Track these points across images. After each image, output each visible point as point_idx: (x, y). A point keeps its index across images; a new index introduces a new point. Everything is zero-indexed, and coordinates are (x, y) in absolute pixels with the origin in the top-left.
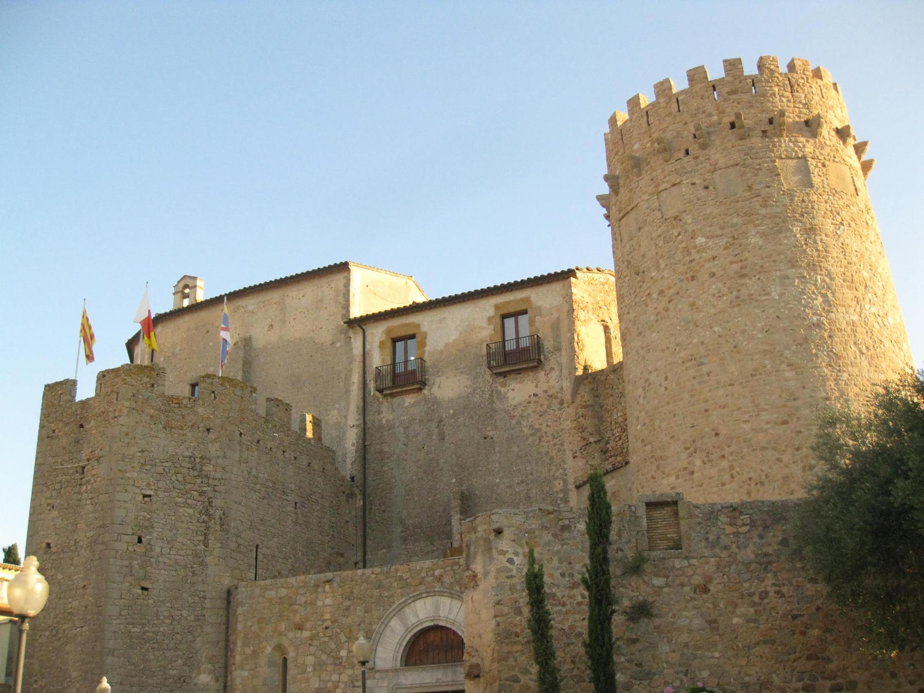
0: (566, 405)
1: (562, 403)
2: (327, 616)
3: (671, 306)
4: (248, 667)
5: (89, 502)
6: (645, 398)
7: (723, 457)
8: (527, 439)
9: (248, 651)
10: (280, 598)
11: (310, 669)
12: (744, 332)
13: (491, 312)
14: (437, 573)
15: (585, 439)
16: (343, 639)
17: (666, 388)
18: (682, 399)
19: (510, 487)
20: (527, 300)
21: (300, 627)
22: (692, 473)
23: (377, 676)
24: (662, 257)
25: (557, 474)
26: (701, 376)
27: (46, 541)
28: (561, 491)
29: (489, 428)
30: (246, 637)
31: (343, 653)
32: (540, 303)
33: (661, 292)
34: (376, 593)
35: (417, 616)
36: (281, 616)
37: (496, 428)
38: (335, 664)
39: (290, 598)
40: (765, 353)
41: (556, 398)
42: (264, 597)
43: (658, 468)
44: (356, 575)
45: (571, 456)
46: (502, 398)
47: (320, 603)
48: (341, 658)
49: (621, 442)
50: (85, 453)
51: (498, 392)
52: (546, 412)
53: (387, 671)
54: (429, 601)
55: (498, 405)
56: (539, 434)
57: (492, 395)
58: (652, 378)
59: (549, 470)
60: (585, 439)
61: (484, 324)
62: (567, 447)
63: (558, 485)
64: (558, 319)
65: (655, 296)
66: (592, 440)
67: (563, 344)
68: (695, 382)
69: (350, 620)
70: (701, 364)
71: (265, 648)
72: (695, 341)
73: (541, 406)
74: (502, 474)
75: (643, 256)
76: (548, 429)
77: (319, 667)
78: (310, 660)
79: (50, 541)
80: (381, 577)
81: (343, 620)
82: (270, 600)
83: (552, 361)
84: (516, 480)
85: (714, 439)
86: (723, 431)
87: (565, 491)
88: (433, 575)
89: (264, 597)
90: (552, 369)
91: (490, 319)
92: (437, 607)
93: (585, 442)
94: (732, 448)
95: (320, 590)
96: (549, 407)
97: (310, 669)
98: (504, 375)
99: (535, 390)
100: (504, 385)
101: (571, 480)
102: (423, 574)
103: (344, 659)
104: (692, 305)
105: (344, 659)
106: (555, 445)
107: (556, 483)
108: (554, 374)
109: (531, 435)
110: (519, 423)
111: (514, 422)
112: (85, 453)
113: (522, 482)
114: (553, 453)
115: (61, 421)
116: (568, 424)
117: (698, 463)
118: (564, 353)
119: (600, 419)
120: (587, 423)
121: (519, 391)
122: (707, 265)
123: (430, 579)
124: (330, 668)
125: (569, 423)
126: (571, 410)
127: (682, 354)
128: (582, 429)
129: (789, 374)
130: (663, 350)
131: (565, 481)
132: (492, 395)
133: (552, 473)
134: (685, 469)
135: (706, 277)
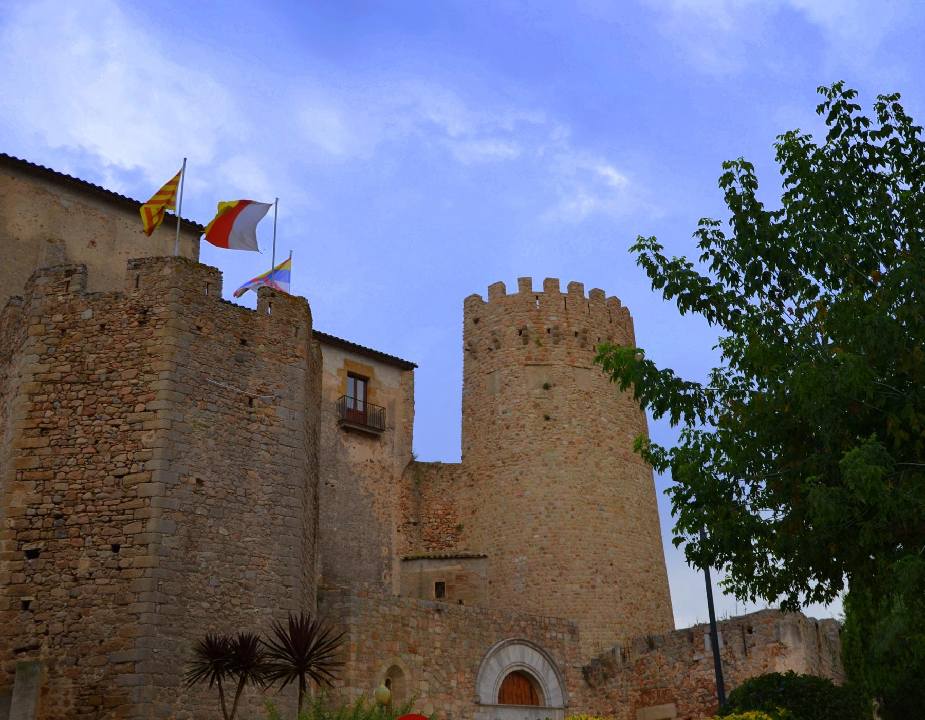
0: (394, 481)
1: (392, 477)
2: (438, 644)
3: (580, 457)
4: (363, 684)
5: (264, 447)
6: (547, 516)
7: (616, 582)
8: (363, 500)
9: (364, 666)
10: (394, 616)
11: (424, 695)
12: (627, 499)
13: (341, 365)
14: (523, 624)
16: (453, 670)
17: (573, 517)
18: (586, 530)
19: (345, 539)
20: (371, 370)
21: (413, 651)
22: (594, 587)
23: (482, 709)
24: (574, 416)
25: (384, 541)
26: (602, 518)
27: (197, 475)
28: (387, 557)
29: (331, 476)
30: (359, 651)
31: (453, 683)
32: (381, 379)
33: (571, 443)
34: (477, 631)
35: (509, 659)
36: (396, 636)
37: (337, 478)
38: (447, 693)
39: (403, 618)
40: (638, 519)
41: (388, 471)
42: (377, 611)
43: (561, 574)
44: (460, 610)
45: (395, 528)
46: (345, 452)
47: (431, 630)
48: (451, 688)
49: (438, 531)
50: (253, 382)
51: (341, 443)
52: (378, 480)
53: (489, 706)
54: (518, 648)
55: (340, 456)
56: (372, 499)
57: (336, 444)
58: (558, 504)
59: (378, 536)
61: (334, 373)
63: (385, 551)
64: (394, 401)
65: (565, 443)
66: (412, 520)
67: (396, 425)
68: (598, 521)
69: (457, 652)
70: (602, 510)
71: (381, 666)
72: (599, 491)
74: (339, 525)
75: (557, 408)
76: (379, 497)
77: (432, 694)
78: (425, 686)
79: (203, 478)
80: (481, 617)
81: (451, 650)
82: (384, 616)
83: (392, 437)
84: (351, 535)
85: (610, 568)
86: (615, 563)
87: (390, 558)
88: (519, 625)
89: (377, 611)
90: (386, 444)
91: (339, 370)
92: (523, 656)
93: (406, 520)
94: (621, 578)
95: (430, 616)
96: (382, 477)
97: (424, 695)
98: (347, 430)
99: (371, 457)
100: (347, 440)
101: (394, 550)
102: (512, 623)
103: (455, 689)
104: (597, 464)
105: (455, 689)
106: (384, 513)
107: (383, 548)
108: (387, 449)
109: (366, 496)
110: (356, 481)
111: (353, 478)
112: (253, 382)
113: (356, 538)
114: (382, 521)
115: (212, 321)
116: (395, 499)
117: (599, 580)
118: (396, 433)
119: (419, 503)
120: (410, 504)
121: (358, 451)
122: (608, 440)
123: (516, 628)
124: (442, 696)
125: (396, 497)
126: (398, 487)
127: (588, 496)
128: (404, 507)
129: (648, 539)
130: (571, 487)
131: (390, 549)
132: (336, 444)
133: (380, 538)
134: (589, 582)
135: (607, 448)
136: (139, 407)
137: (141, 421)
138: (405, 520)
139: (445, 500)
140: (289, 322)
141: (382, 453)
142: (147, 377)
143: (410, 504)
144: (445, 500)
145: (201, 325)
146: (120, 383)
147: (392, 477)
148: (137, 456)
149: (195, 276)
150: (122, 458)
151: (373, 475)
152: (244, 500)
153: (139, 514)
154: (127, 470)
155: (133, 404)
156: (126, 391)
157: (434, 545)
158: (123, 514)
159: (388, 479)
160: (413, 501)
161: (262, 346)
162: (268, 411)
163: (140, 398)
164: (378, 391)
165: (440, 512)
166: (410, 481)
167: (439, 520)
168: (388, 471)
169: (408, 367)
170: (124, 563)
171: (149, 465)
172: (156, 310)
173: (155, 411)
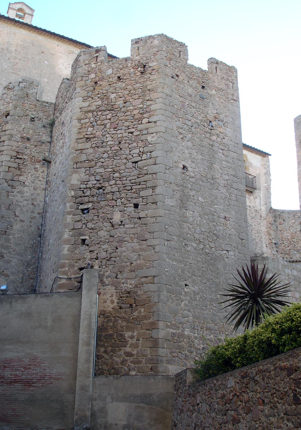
15: (270, 240)
27: (183, 163)
32: (251, 161)
45: (265, 245)
60: (270, 240)
62: (263, 240)
73: (252, 213)
76: (255, 227)
83: (260, 193)
96: (256, 215)
108: (258, 201)
114: (257, 240)
115: (184, 72)
116: (263, 229)
118: (262, 192)
120: (272, 232)
125: (264, 228)
126: (265, 222)
136: (145, 121)
137: (147, 129)
138: (270, 241)
139: (292, 230)
140: (228, 79)
141: (255, 203)
142: (149, 103)
143: (272, 232)
144: (292, 230)
145: (178, 74)
146: (132, 108)
147: (261, 216)
148: (146, 149)
149: (173, 46)
150: (137, 151)
151: (251, 214)
152: (212, 181)
153: (149, 184)
154: (140, 158)
155: (140, 119)
156: (136, 112)
157: (287, 256)
158: (139, 185)
159: (259, 218)
160: (274, 231)
161: (214, 91)
162: (221, 130)
163: (145, 116)
164: (250, 168)
165: (289, 237)
166: (271, 219)
167: (288, 242)
168: (258, 213)
169: (264, 154)
170: (142, 215)
171: (154, 154)
172: (151, 65)
173: (155, 122)
